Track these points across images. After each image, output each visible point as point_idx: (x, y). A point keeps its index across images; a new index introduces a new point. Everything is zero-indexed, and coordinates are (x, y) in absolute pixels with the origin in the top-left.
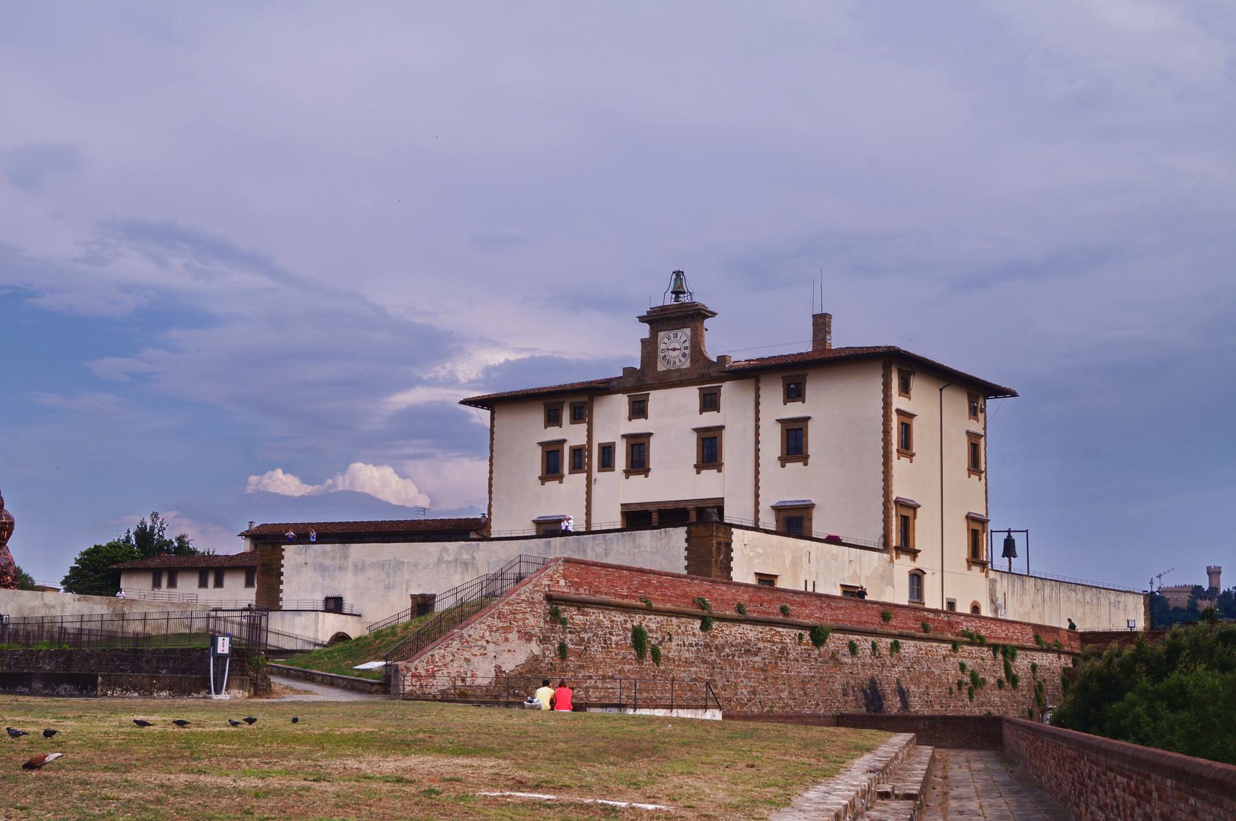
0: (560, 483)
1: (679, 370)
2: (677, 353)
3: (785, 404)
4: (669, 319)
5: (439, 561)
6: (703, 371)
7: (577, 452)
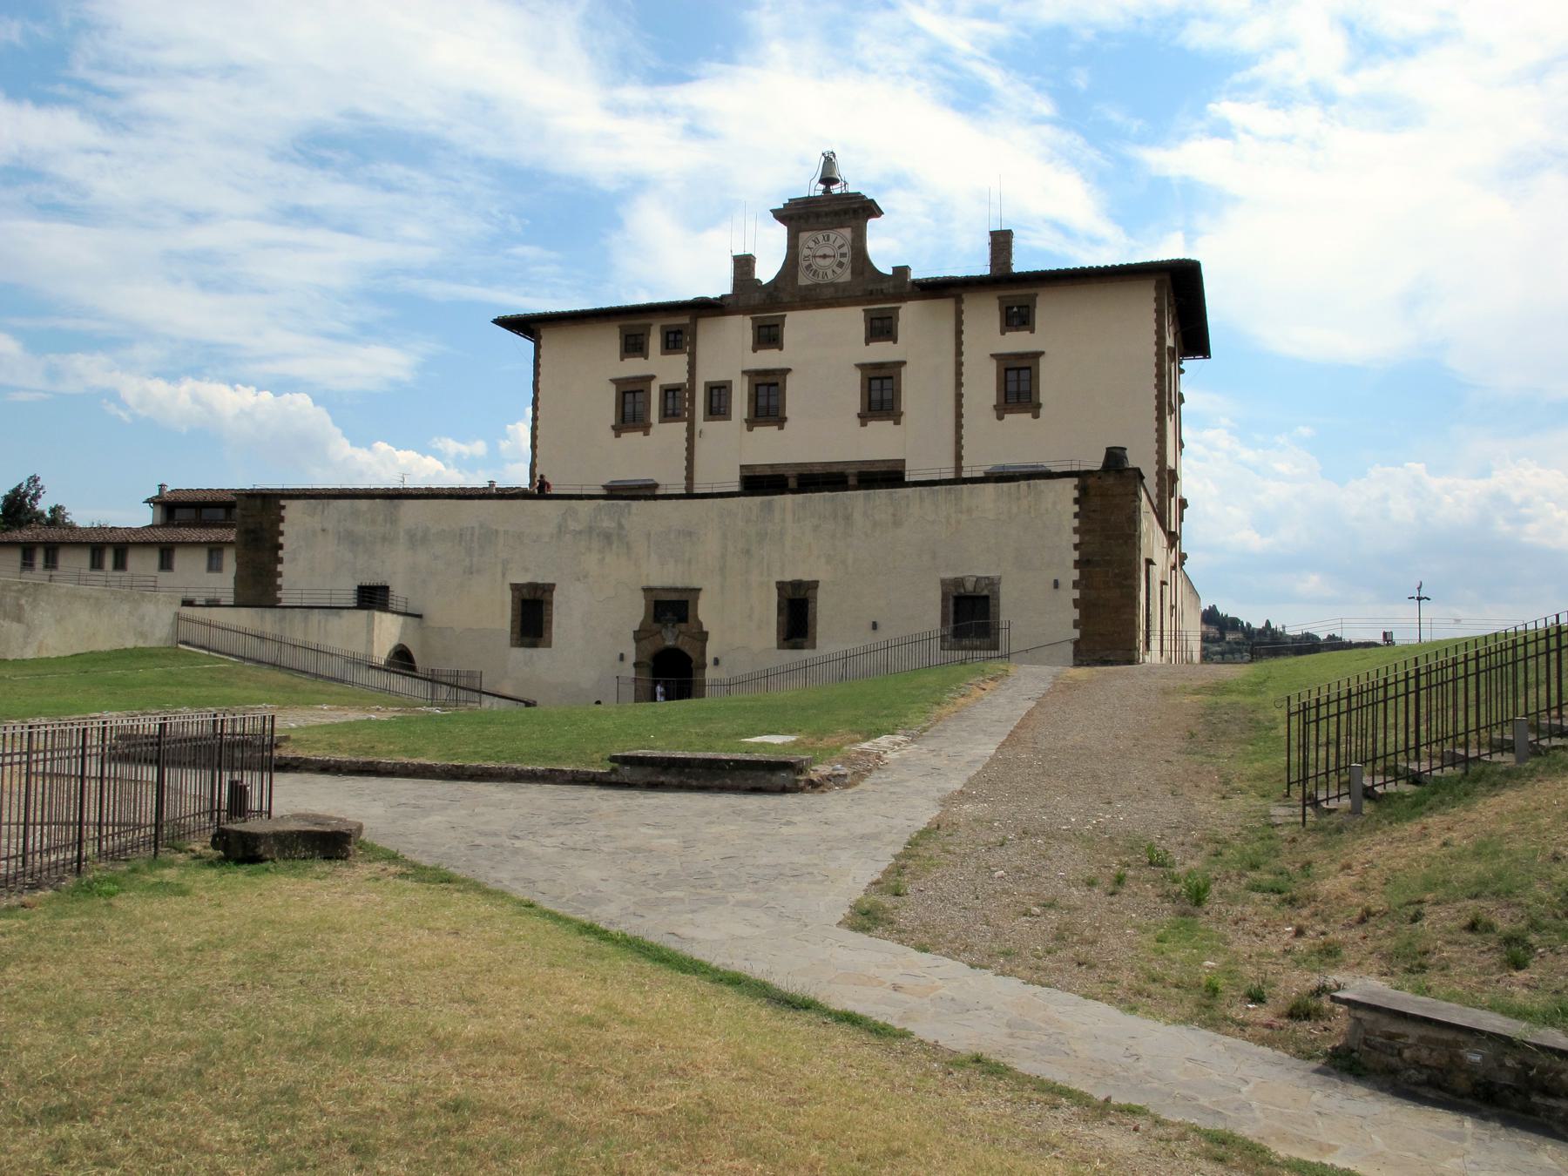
0: (645, 435)
1: (833, 285)
2: (828, 262)
3: (1003, 333)
4: (818, 215)
5: (560, 531)
6: (870, 287)
7: (669, 392)
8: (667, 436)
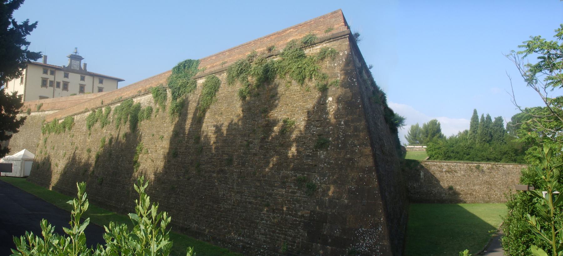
8: (50, 89)
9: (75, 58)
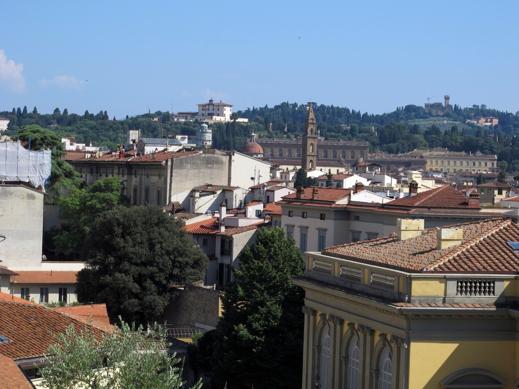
8: (204, 111)
9: (211, 101)
